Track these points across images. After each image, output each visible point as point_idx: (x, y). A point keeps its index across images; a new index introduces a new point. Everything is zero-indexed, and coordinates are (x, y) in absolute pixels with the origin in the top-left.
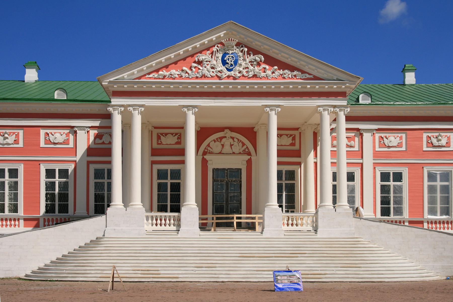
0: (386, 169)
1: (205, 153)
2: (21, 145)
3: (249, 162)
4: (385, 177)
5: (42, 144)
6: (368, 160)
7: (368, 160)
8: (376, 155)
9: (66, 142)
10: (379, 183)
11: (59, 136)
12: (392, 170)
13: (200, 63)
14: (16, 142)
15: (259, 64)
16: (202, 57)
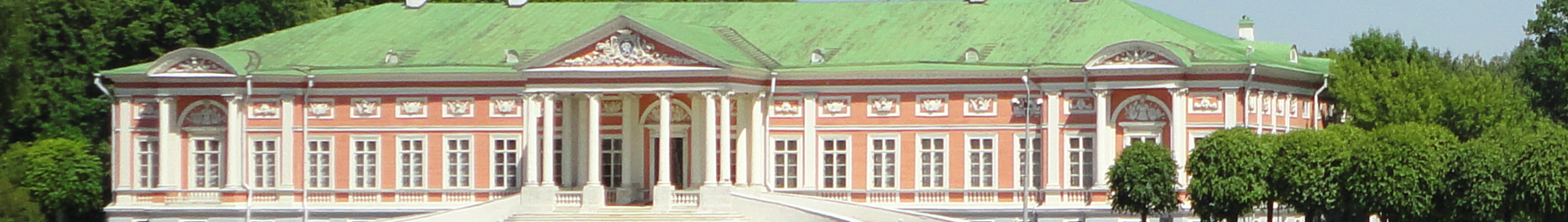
0: (829, 137)
1: (647, 122)
2: (471, 115)
3: (689, 131)
4: (829, 145)
5: (492, 114)
6: (810, 126)
7: (810, 126)
8: (820, 121)
9: (514, 112)
10: (822, 151)
11: (507, 105)
12: (835, 138)
13: (601, 51)
14: (468, 111)
15: (651, 52)
16: (601, 46)
